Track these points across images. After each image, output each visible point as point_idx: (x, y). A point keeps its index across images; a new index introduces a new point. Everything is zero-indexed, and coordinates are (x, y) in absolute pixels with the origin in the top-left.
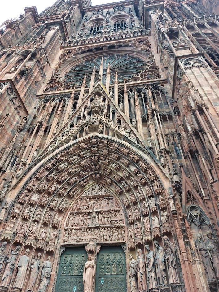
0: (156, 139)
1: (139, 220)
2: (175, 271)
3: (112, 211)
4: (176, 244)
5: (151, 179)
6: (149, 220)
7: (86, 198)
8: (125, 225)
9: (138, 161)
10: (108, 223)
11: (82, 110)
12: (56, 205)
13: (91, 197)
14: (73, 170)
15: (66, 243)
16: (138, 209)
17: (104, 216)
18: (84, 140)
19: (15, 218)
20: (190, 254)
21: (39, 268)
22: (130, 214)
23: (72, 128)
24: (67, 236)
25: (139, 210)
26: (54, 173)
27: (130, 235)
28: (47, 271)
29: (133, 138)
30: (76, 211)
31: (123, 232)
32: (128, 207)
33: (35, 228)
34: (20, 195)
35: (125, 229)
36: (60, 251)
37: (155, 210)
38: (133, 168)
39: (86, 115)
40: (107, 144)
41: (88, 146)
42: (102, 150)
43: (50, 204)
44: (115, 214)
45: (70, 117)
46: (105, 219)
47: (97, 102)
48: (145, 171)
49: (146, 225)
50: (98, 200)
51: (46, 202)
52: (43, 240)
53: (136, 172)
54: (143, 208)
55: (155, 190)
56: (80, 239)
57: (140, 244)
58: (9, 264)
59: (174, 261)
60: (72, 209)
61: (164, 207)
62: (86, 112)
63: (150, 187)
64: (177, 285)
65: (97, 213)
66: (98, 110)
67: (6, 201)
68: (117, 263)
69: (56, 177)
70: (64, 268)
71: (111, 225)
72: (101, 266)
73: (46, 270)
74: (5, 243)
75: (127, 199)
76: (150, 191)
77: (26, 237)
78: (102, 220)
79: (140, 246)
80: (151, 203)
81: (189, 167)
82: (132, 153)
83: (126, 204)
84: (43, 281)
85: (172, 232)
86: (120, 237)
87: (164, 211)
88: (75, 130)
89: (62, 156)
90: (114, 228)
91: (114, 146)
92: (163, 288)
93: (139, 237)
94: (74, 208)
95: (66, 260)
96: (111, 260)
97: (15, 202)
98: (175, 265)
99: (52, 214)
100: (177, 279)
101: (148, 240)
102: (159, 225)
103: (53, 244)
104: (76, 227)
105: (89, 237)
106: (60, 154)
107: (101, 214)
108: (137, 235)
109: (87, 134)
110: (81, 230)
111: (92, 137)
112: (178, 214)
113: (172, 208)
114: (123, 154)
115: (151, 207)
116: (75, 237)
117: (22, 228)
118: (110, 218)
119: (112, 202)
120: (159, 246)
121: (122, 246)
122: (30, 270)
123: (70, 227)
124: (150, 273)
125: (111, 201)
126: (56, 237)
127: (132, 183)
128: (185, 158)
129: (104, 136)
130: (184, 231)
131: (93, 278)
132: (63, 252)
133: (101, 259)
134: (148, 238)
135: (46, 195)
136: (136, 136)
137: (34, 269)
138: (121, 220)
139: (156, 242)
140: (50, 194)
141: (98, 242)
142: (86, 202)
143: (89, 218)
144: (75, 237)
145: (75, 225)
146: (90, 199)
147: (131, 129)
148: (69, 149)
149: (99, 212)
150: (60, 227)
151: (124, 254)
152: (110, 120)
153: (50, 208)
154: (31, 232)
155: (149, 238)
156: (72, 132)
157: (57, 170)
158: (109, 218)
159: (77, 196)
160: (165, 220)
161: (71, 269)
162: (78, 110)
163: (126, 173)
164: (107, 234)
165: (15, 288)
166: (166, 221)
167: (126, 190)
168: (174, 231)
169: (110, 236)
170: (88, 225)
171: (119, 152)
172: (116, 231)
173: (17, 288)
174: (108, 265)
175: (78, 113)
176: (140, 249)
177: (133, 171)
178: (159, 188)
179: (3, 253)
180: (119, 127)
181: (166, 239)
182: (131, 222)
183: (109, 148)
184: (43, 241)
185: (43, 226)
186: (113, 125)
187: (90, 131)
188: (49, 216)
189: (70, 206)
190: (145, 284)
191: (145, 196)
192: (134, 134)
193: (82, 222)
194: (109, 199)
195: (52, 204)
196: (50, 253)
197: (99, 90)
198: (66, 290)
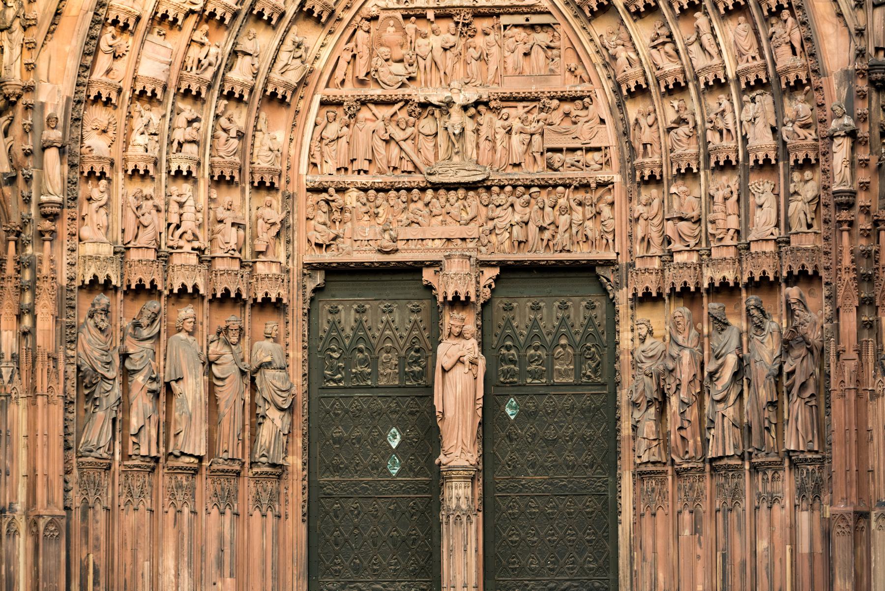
1: (688, 174)
2: (808, 414)
3: (552, 98)
4: (829, 320)
6: (735, 197)
7: (398, 14)
8: (617, 178)
10: (529, 159)
12: (255, 76)
13: (430, 15)
15: (327, 257)
16: (691, 125)
17: (506, 123)
19: (103, 182)
20: (871, 365)
21: (243, 373)
22: (647, 135)
24: (325, 224)
25: (695, 127)
27: (639, 231)
28: (279, 384)
30: (350, 91)
31: (606, 211)
32: (641, 91)
33: (189, 213)
34: (90, 59)
35: (617, 194)
36: (304, 287)
37: (767, 161)
43: (224, 80)
44: (567, 115)
46: (516, 139)
49: (720, 215)
50: (465, 30)
51: (208, 75)
52: (232, 258)
55: (780, 66)
56: (394, 240)
58: (140, 378)
59: (812, 381)
60: (326, 77)
61: (807, 160)
63: (756, 33)
64: (809, 456)
65: (472, 111)
67: (43, 105)
68: (578, 338)
70: (331, 357)
71: (549, 175)
72: (503, 351)
73: (270, 380)
74: (104, 299)
75: (633, 56)
76: (754, 58)
77: (164, 258)
78: (499, 147)
80: (753, 121)
83: (626, 79)
84: (267, 423)
85: (823, 273)
86: (590, 234)
87: (808, 174)
90: (560, 189)
92: (759, 460)
94: (339, 75)
95: (334, 325)
96: (550, 326)
97: (79, 102)
98: (812, 395)
100: (810, 438)
101: (724, 284)
102: (776, 231)
104: (363, 179)
105: (436, 229)
107: (490, 109)
108: (676, 246)
110: (393, 193)
112: (857, 208)
113: (837, 179)
115: (752, 143)
116: (368, 229)
117: (145, 220)
118: (542, 134)
119: (549, 47)
120: (764, 316)
121: (599, 271)
122: (211, 389)
123: (327, 174)
124: (720, 406)
125: (542, 38)
126: (278, 234)
130: (866, 279)
131: (475, 404)
132: (316, 290)
133: (503, 324)
134: (724, 278)
135: (198, 36)
137: (227, 381)
138: (598, 149)
139: (753, 299)
141: (484, 257)
142: (398, 37)
143: (426, 131)
144: (368, 229)
145: (356, 166)
146: (422, 17)
149: (477, 104)
150: (288, 182)
151: (612, 303)
154: (180, 231)
155: (730, 278)
158: (537, 138)
159: (347, 8)
160: (804, 222)
161: (363, 362)
164: (526, 219)
165: (183, 454)
166: (809, 226)
167: (633, 9)
168: (833, 271)
169: (542, 229)
170: (430, 174)
172: (573, 205)
173: (191, 455)
174: (537, 348)
176: (687, 310)
178: (800, 61)
179: (102, 337)
181: (793, 301)
182: (652, 177)
184: (236, 266)
188: (235, 143)
189: (319, 65)
190: (694, 436)
191: (731, 74)
193: (394, 150)
194: (532, 27)
195: (233, 75)
198: (359, 442)
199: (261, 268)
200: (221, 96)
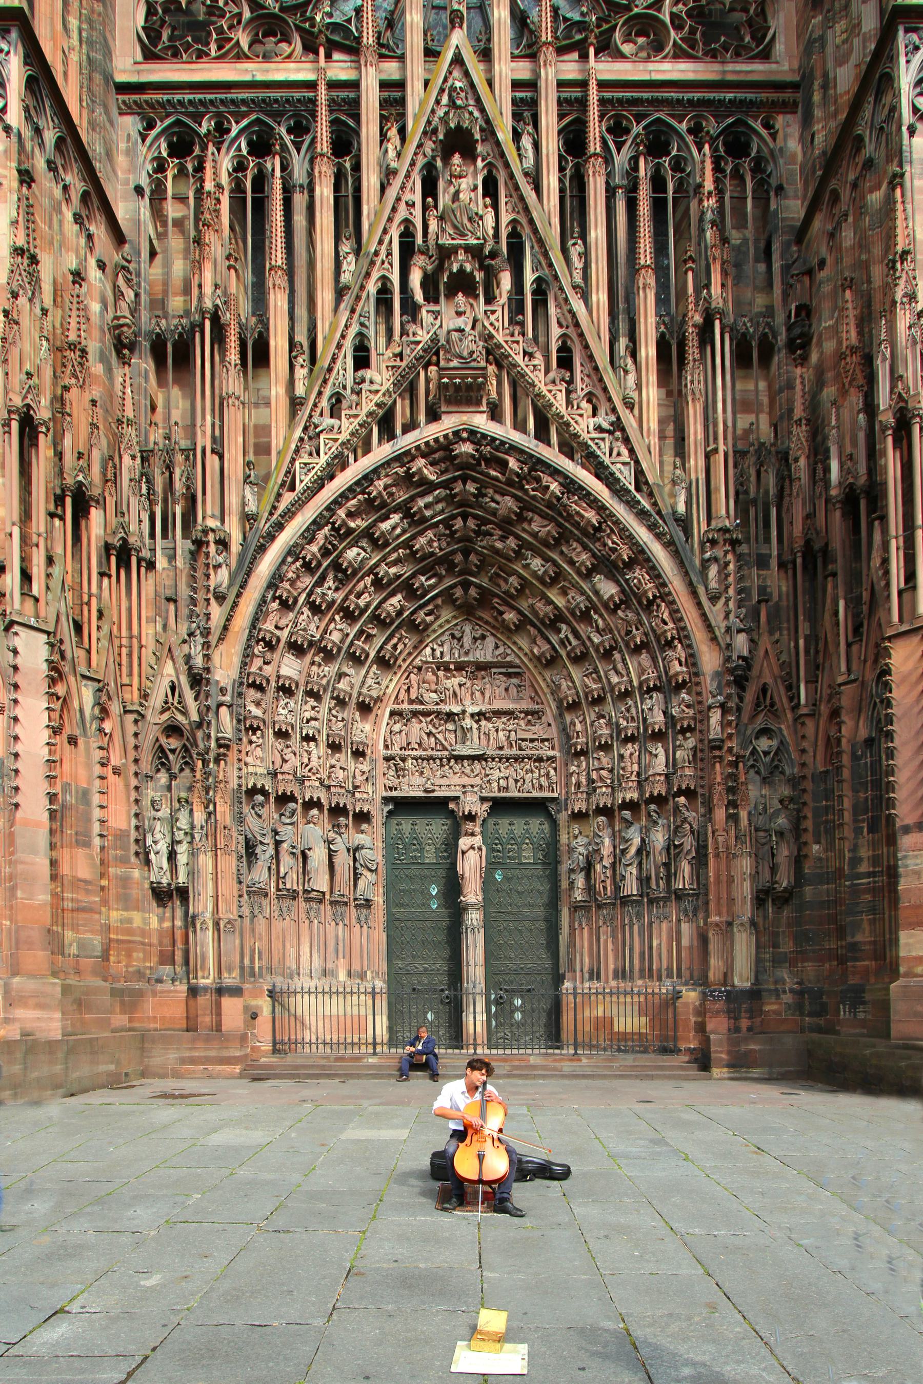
0: (702, 476)
5: (666, 638)
9: (630, 564)
11: (389, 254)
14: (393, 570)
18: (427, 443)
23: (368, 374)
29: (624, 464)
38: (608, 589)
39: (419, 297)
40: (518, 475)
41: (442, 473)
45: (348, 300)
47: (466, 221)
48: (650, 606)
53: (615, 604)
54: (624, 718)
57: (605, 806)
62: (416, 278)
69: (339, 597)
79: (605, 811)
81: (784, 603)
82: (612, 531)
88: (384, 389)
91: (548, 487)
93: (604, 789)
99: (345, 716)
103: (365, 796)
109: (433, 416)
111: (456, 433)
114: (577, 525)
127: (597, 640)
128: (782, 565)
129: (504, 431)
136: (632, 451)
140: (329, 656)
147: (614, 410)
148: (371, 482)
152: (530, 350)
153: (337, 698)
156: (377, 398)
157: (336, 566)
162: (376, 253)
163: (580, 599)
171: (560, 515)
175: (375, 275)
177: (606, 598)
180: (569, 392)
183: (526, 492)
185: (329, 752)
186: (541, 375)
187: (449, 402)
188: (341, 724)
191: (635, 683)
192: (626, 441)
195: (340, 686)
196: (363, 817)
197: (466, 125)
199: (357, 795)
200: (332, 698)
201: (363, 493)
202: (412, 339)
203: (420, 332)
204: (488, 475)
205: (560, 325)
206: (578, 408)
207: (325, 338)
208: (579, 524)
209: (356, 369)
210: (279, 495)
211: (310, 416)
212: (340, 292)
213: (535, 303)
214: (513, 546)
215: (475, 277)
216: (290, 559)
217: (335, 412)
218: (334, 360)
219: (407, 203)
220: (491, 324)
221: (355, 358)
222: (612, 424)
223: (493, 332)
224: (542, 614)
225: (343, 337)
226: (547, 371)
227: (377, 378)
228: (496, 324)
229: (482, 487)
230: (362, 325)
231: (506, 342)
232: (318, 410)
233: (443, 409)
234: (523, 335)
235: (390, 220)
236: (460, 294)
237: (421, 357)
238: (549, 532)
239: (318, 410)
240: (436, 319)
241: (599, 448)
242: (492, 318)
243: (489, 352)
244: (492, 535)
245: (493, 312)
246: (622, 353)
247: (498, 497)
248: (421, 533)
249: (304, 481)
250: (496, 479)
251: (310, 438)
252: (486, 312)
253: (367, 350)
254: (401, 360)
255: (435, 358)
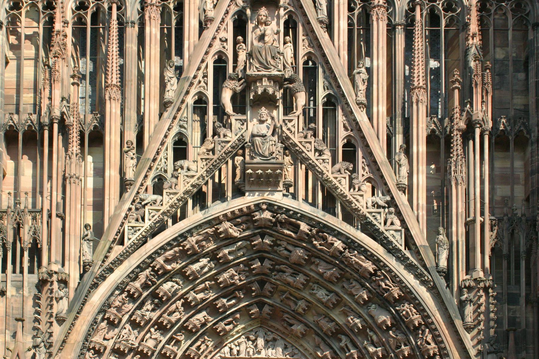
18: (233, 213)
23: (185, 163)
26: (149, 306)
39: (229, 108)
42: (290, 248)
47: (269, 59)
66: (273, 95)
89: (167, 261)
106: (159, 255)
148: (186, 238)
152: (320, 148)
201: (178, 245)
202: (222, 139)
203: (229, 134)
204: (283, 234)
205: (346, 129)
206: (359, 190)
207: (150, 137)
208: (358, 270)
209: (176, 159)
210: (111, 248)
211: (138, 193)
212: (164, 105)
213: (325, 112)
214: (302, 280)
215: (276, 96)
216: (117, 292)
217: (158, 189)
218: (158, 153)
219: (220, 39)
220: (289, 129)
221: (175, 150)
222: (387, 202)
223: (290, 135)
224: (325, 329)
225: (166, 136)
226: (334, 163)
227: (193, 167)
228: (293, 129)
229: (277, 240)
230: (181, 126)
231: (300, 142)
232: (144, 188)
233: (247, 188)
234: (315, 137)
235: (207, 53)
236: (263, 108)
237: (230, 152)
238: (333, 273)
239: (144, 188)
240: (243, 124)
241: (376, 219)
242: (290, 125)
243: (285, 149)
244: (284, 272)
245: (290, 121)
246: (397, 151)
247: (290, 248)
248: (225, 270)
249: (131, 239)
250: (290, 236)
251: (137, 209)
252: (284, 121)
253: (186, 144)
254: (214, 154)
255: (241, 152)
